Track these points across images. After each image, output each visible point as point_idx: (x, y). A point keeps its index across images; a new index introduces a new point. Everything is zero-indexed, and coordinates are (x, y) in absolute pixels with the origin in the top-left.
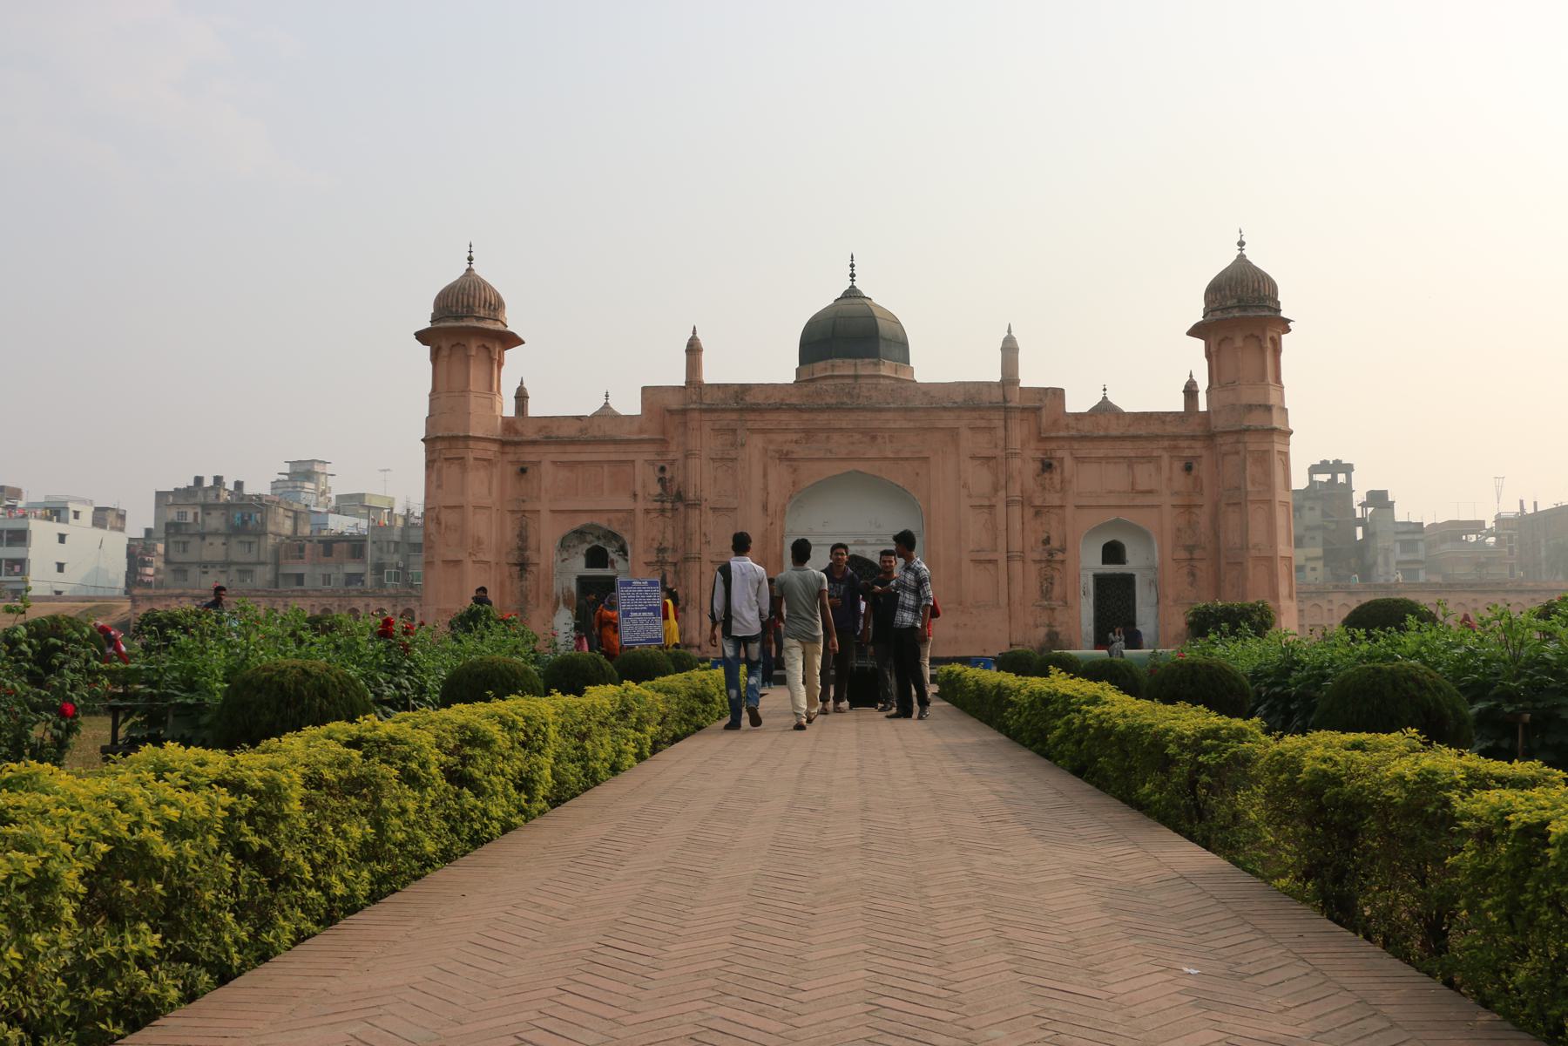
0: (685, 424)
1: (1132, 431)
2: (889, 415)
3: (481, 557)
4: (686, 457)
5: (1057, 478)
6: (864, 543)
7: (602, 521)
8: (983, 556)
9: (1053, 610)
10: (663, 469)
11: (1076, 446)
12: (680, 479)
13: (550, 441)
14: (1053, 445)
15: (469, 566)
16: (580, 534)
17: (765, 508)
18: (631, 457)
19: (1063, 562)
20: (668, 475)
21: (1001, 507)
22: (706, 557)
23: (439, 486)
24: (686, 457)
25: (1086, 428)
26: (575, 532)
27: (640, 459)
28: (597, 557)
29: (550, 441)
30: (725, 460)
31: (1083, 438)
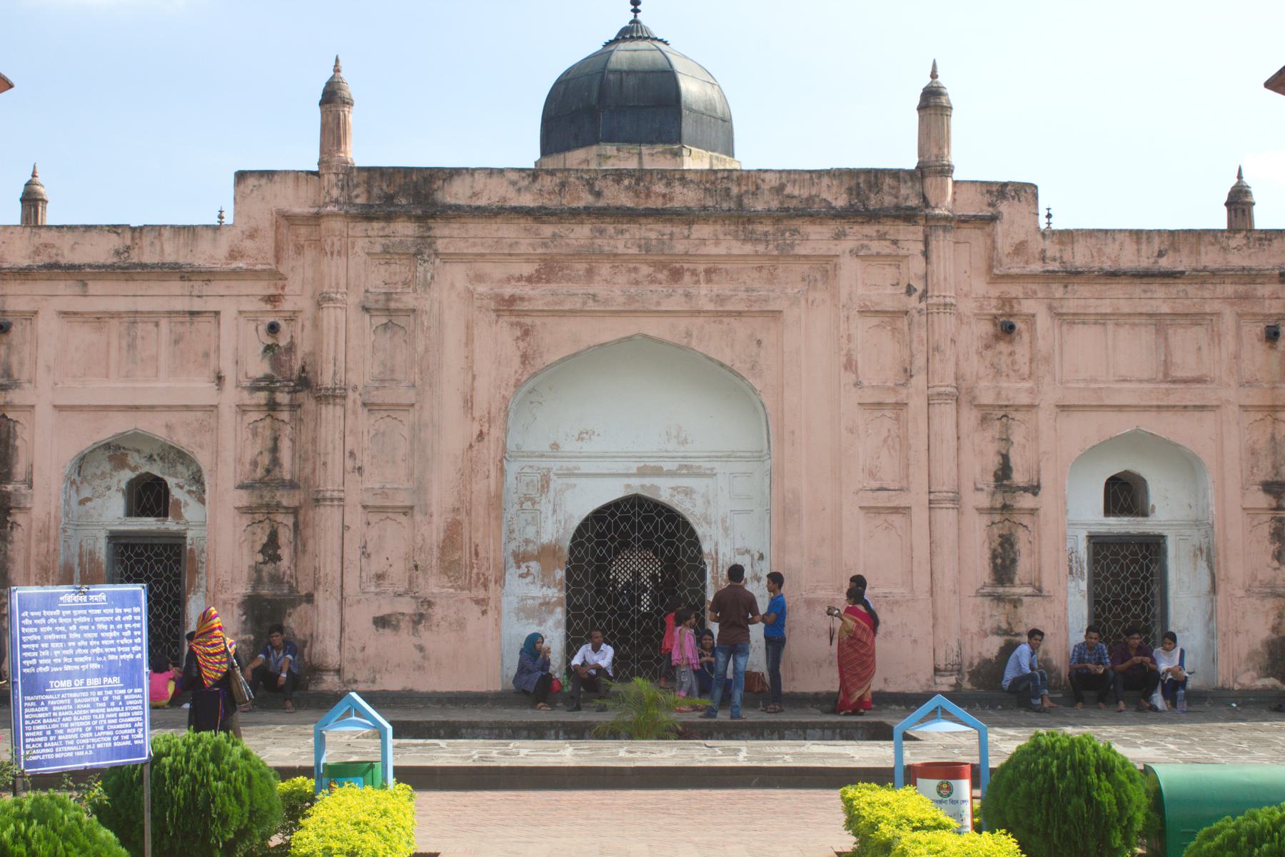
0: (318, 243)
1: (1165, 263)
2: (702, 230)
4: (319, 306)
5: (1022, 350)
6: (658, 472)
7: (154, 426)
8: (882, 499)
9: (1016, 602)
10: (273, 329)
11: (1058, 291)
12: (303, 348)
13: (55, 270)
14: (1015, 290)
16: (115, 451)
17: (469, 403)
18: (212, 305)
19: (1033, 512)
20: (283, 342)
21: (917, 403)
22: (354, 497)
24: (319, 306)
25: (1080, 257)
26: (107, 446)
27: (229, 310)
28: (149, 496)
29: (55, 270)
30: (388, 313)
31: (1072, 275)
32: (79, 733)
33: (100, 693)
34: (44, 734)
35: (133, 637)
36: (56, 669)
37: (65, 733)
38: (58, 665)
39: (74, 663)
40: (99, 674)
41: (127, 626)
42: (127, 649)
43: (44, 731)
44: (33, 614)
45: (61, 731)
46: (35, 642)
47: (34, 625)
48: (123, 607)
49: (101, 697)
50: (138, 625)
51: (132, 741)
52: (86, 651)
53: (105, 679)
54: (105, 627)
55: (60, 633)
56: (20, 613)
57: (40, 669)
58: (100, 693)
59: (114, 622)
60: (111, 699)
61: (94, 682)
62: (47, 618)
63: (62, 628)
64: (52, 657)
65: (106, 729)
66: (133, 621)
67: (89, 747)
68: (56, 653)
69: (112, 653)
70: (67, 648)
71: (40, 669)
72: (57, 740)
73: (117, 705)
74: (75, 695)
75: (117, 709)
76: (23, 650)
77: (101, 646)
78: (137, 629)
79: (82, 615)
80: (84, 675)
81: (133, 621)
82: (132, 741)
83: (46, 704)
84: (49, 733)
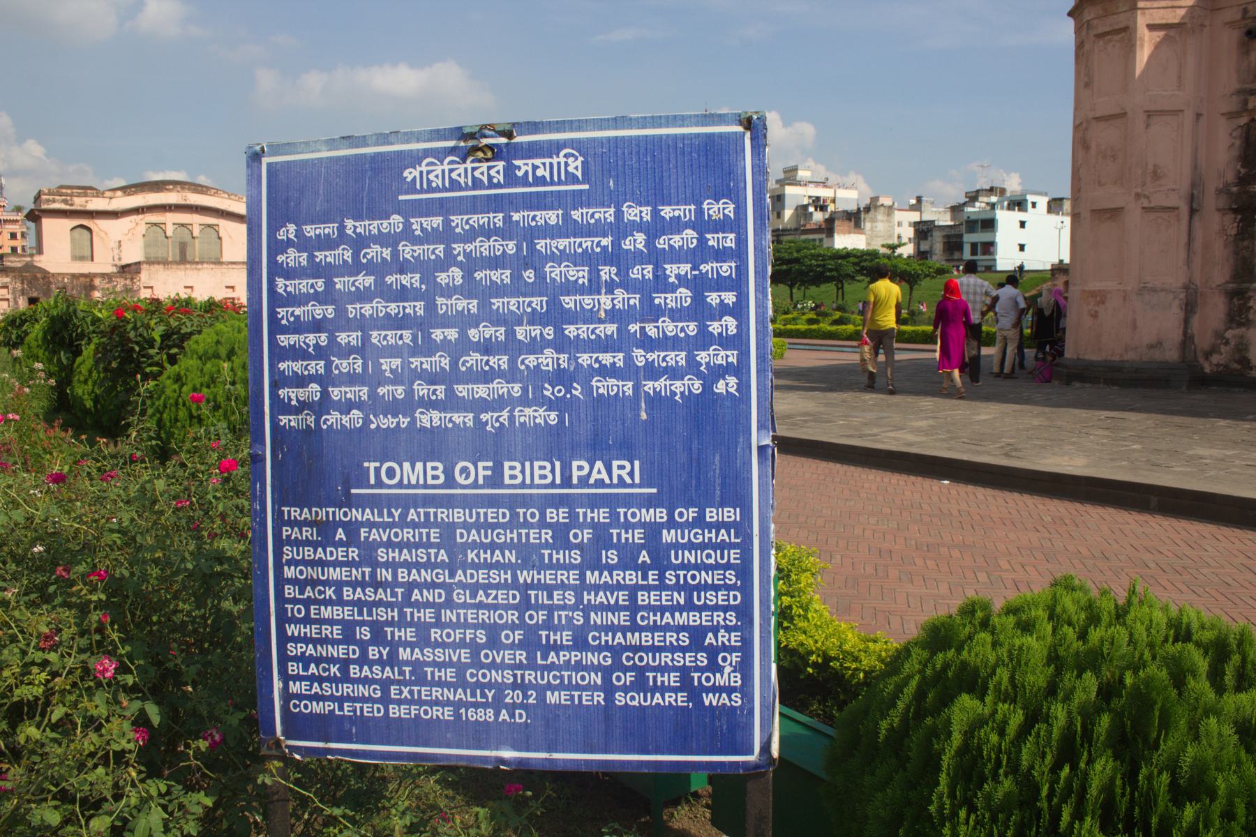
3: (1159, 200)
15: (1134, 216)
23: (1087, 85)
32: (475, 648)
33: (552, 515)
34: (348, 637)
35: (699, 311)
36: (387, 422)
37: (423, 641)
38: (394, 408)
39: (452, 403)
40: (554, 444)
41: (672, 270)
42: (678, 358)
43: (349, 629)
44: (310, 231)
45: (409, 634)
46: (317, 326)
47: (316, 270)
48: (658, 197)
49: (561, 538)
50: (727, 268)
51: (695, 693)
52: (502, 361)
53: (579, 467)
54: (580, 274)
55: (403, 294)
56: (273, 230)
57: (333, 418)
58: (557, 515)
59: (616, 257)
60: (602, 537)
61: (542, 473)
62: (359, 243)
63: (412, 280)
64: (372, 379)
65: (580, 643)
66: (701, 253)
67: (512, 696)
68: (389, 364)
69: (607, 372)
70: (429, 348)
71: (333, 418)
72: (392, 661)
73: (628, 561)
74: (458, 515)
75: (631, 577)
76: (279, 354)
77: (561, 344)
78: (721, 284)
79: (488, 232)
80: (494, 447)
81: (701, 253)
82: (695, 693)
83: (352, 539)
84: (364, 633)
